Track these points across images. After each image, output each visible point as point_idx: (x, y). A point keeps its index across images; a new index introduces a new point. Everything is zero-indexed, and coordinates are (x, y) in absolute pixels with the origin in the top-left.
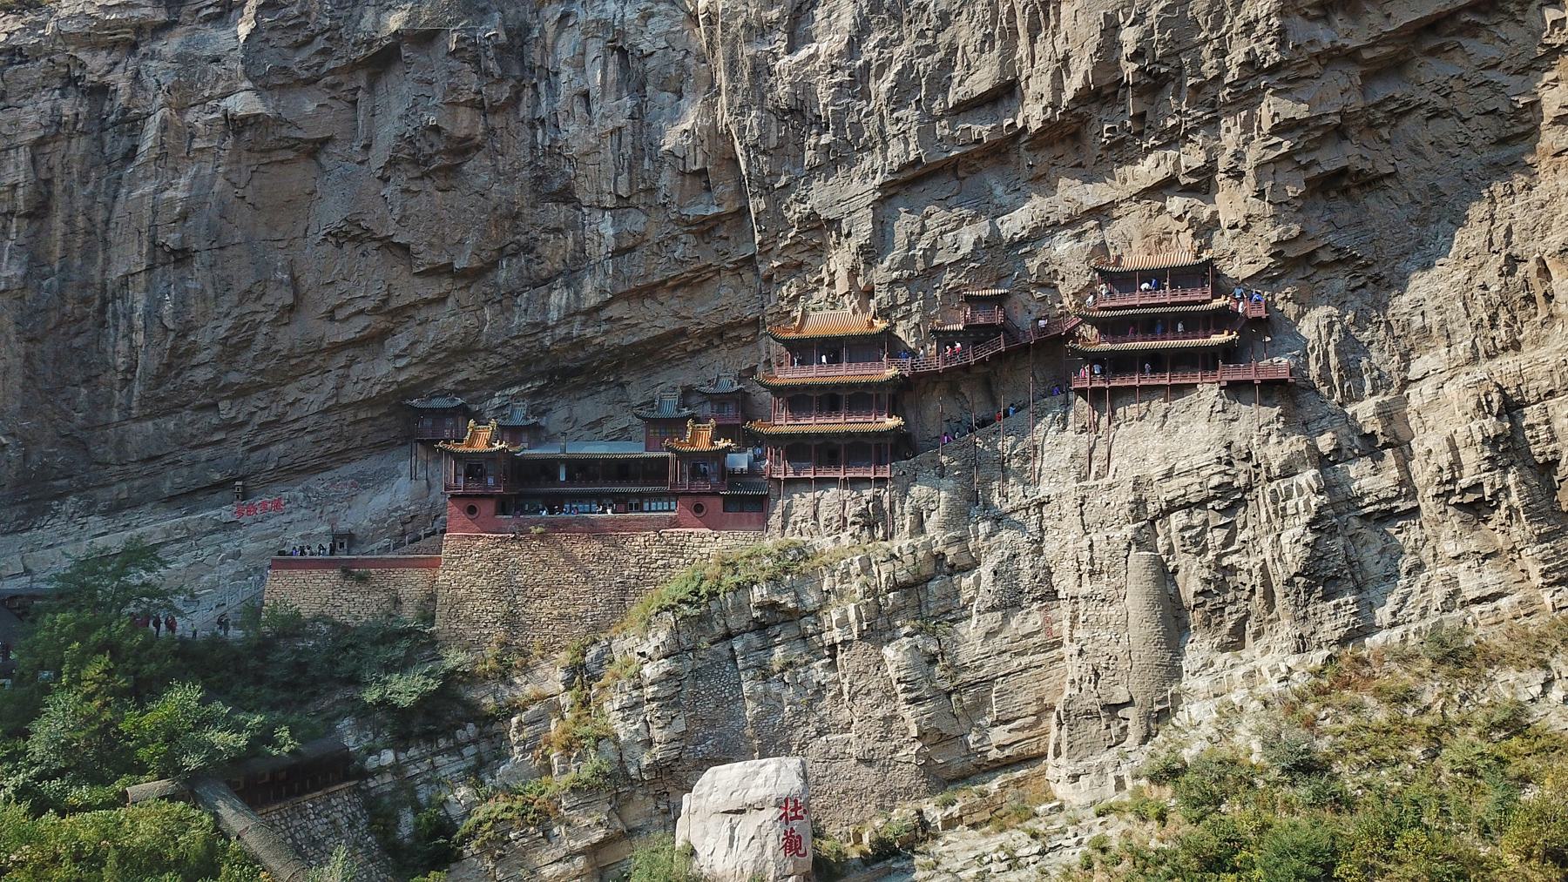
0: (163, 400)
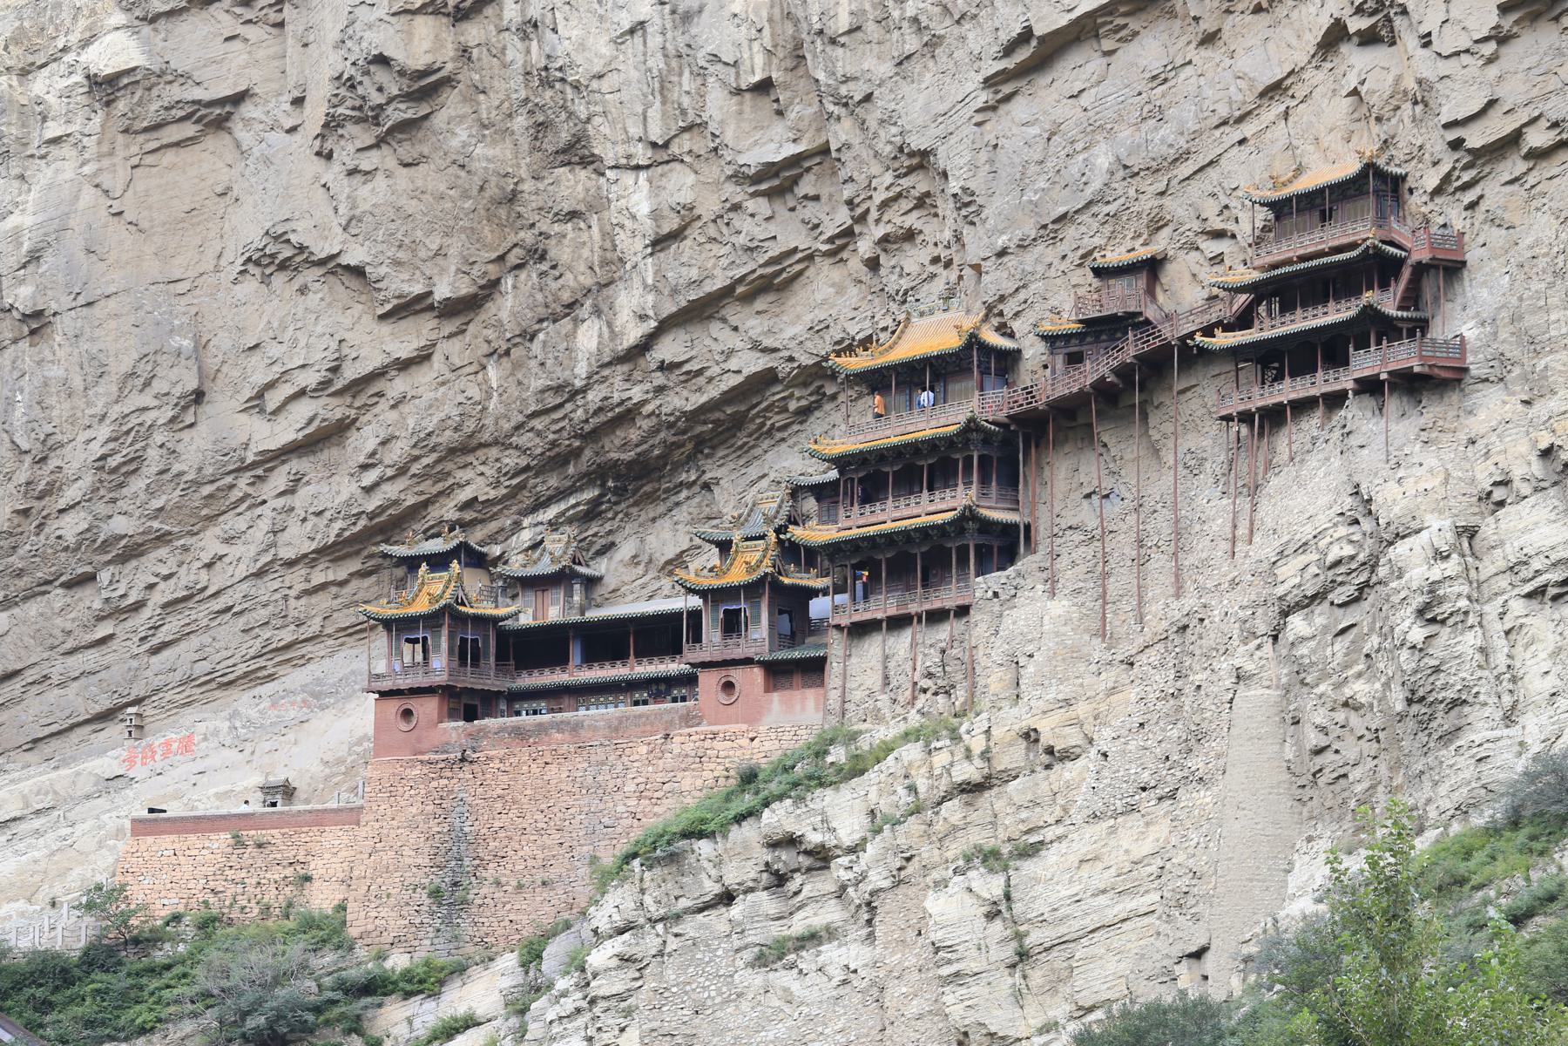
0: (20, 573)
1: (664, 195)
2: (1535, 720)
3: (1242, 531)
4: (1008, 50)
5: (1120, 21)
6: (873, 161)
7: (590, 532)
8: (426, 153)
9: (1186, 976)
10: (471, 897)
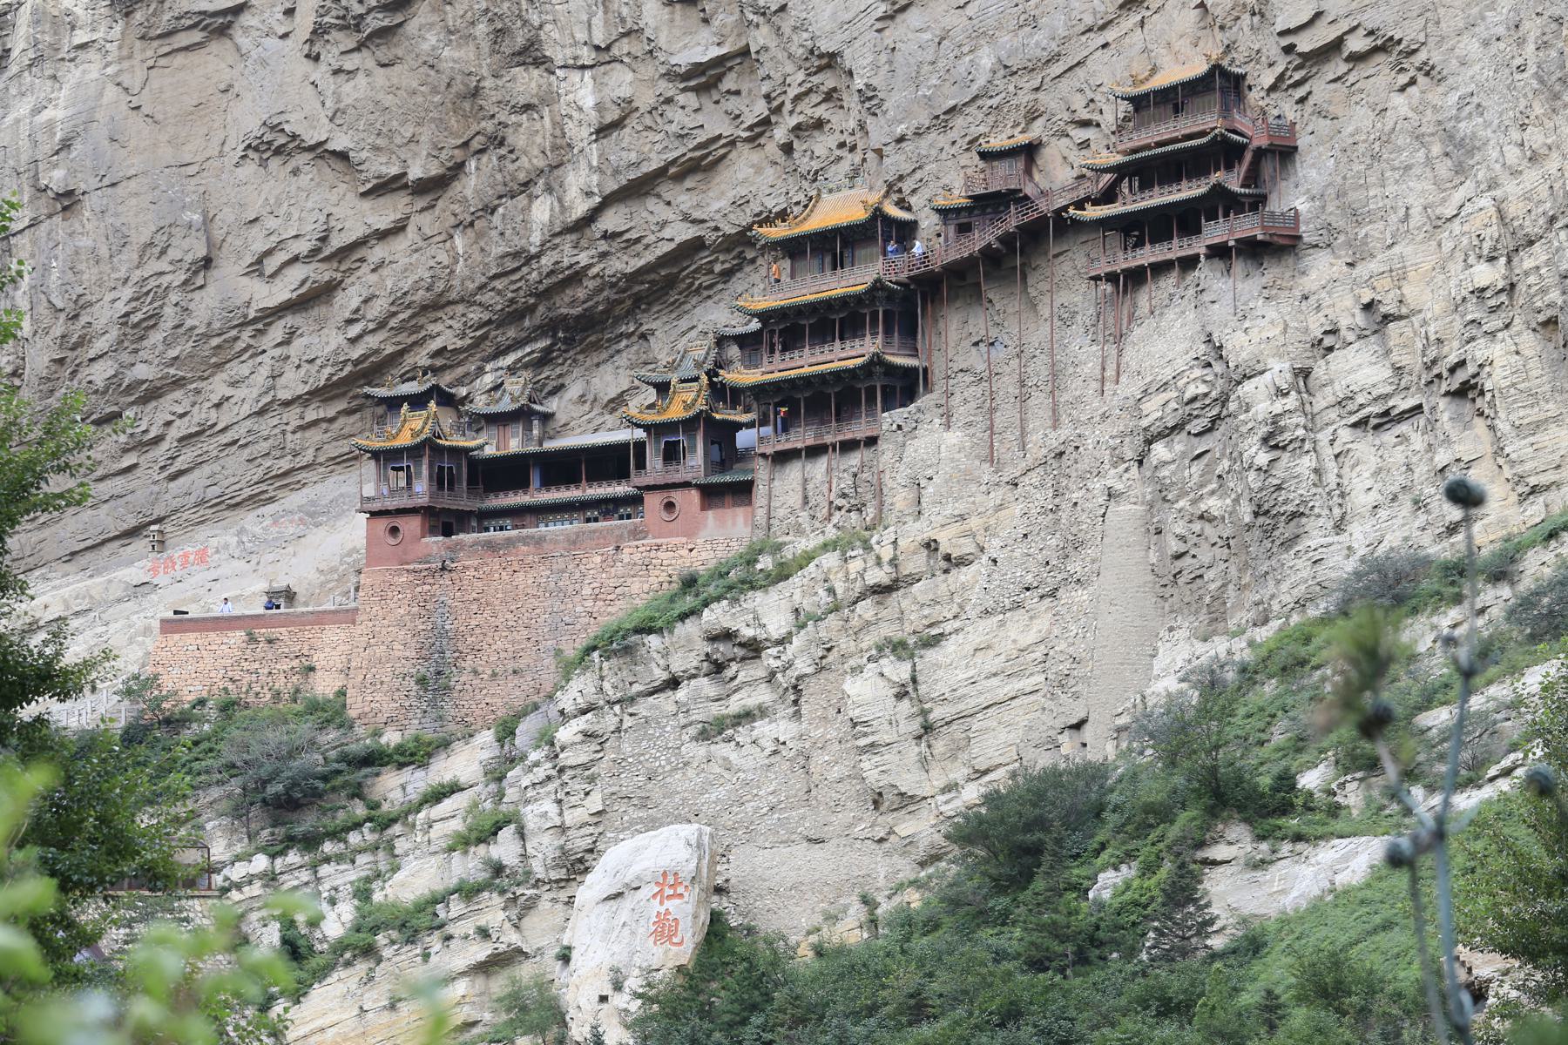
1: (607, 90)
2: (1360, 528)
3: (1110, 373)
6: (787, 62)
7: (543, 376)
8: (400, 55)
9: (1068, 744)
10: (452, 683)
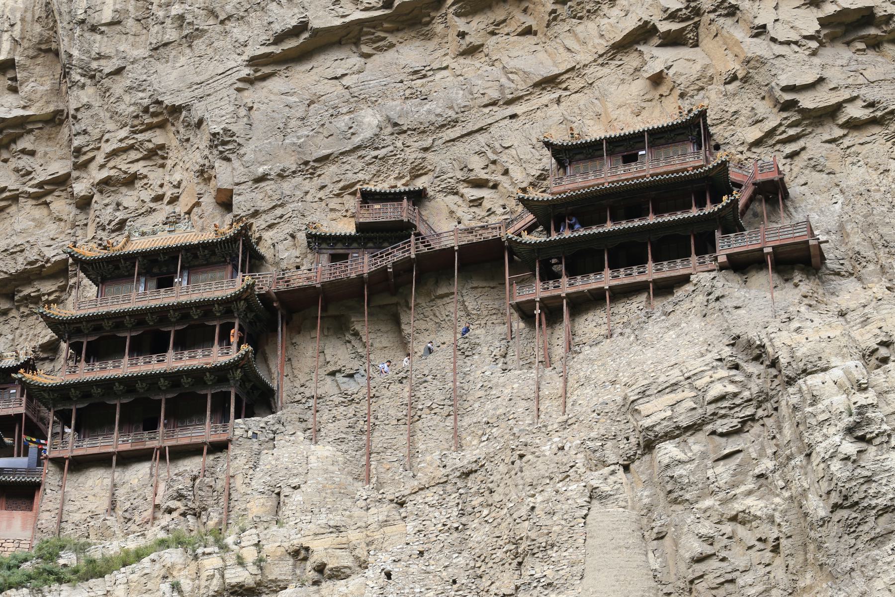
4: (279, 39)
5: (383, 35)
